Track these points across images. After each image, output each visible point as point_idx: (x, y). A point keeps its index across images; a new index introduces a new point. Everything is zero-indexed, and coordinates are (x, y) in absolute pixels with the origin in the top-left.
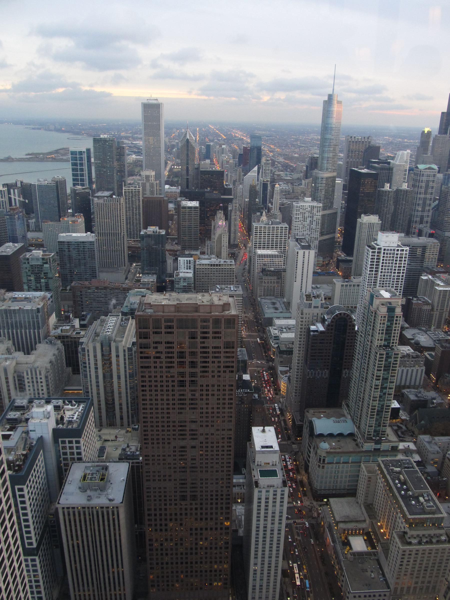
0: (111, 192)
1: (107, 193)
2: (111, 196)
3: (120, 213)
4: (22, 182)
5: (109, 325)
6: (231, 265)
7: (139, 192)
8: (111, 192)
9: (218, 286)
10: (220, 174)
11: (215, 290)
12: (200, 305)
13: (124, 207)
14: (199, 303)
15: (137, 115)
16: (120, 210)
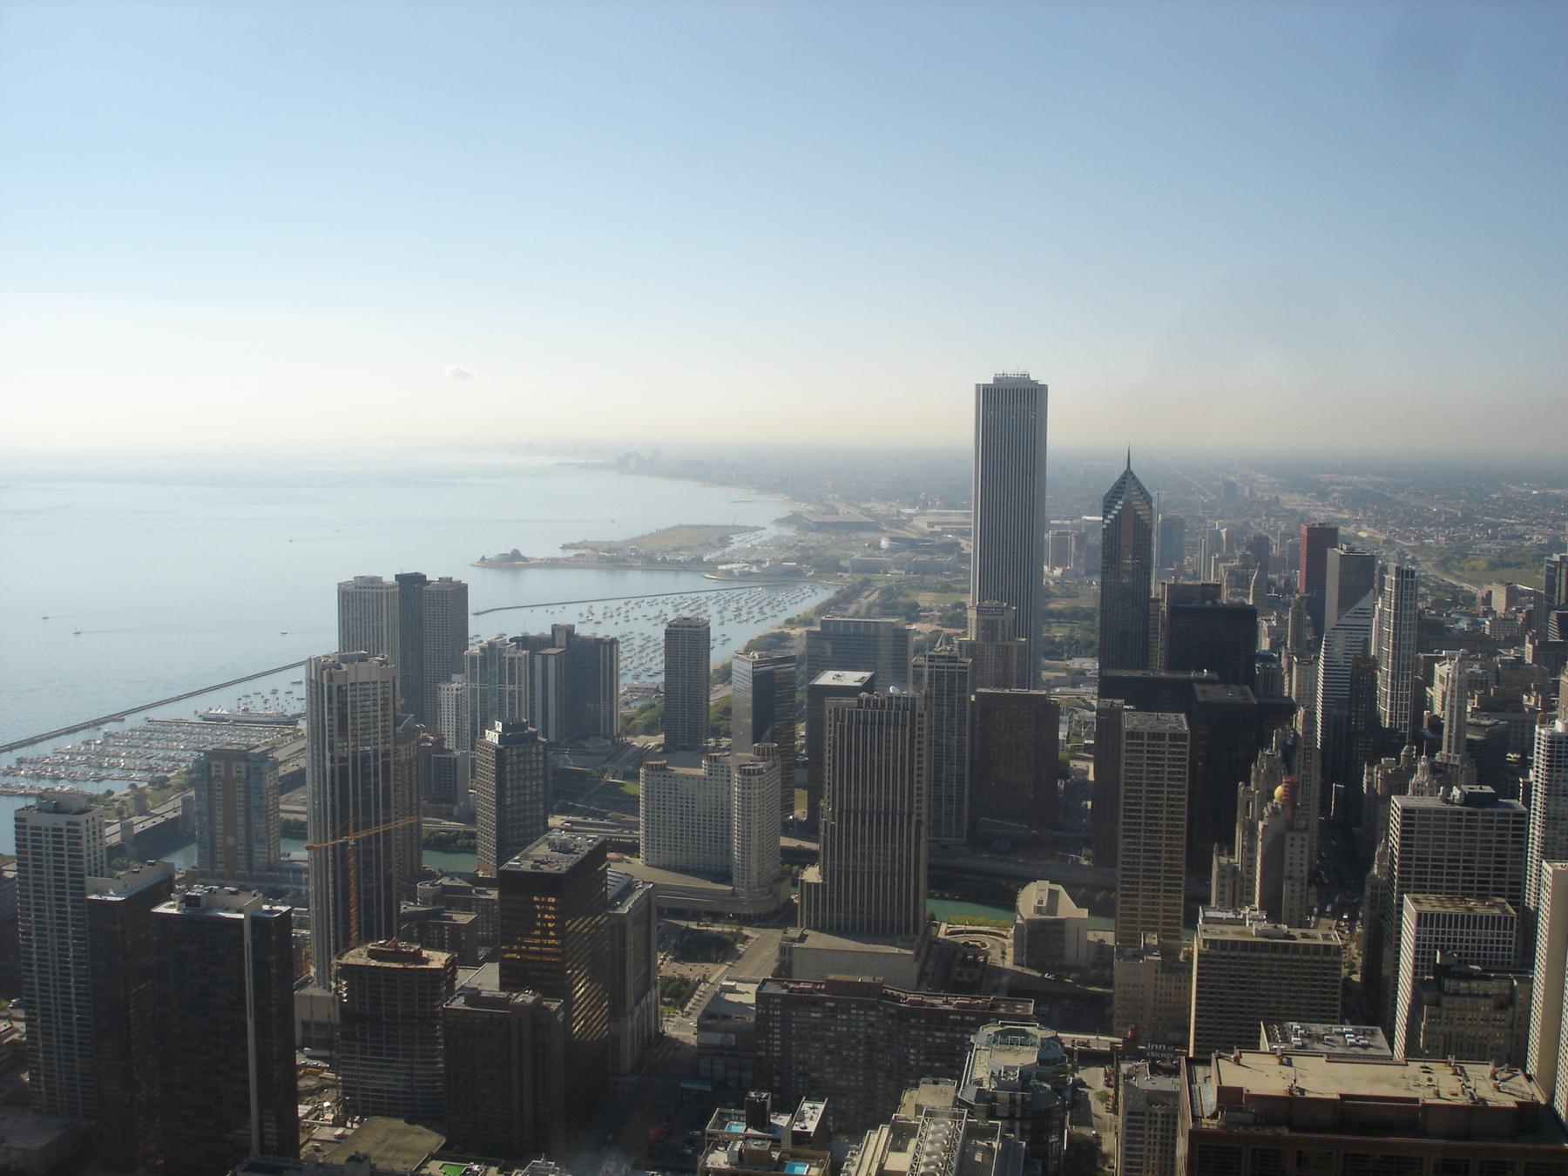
0: (868, 675)
1: (851, 678)
2: (869, 686)
3: (912, 746)
4: (569, 631)
5: (928, 1148)
6: (1327, 948)
7: (963, 676)
8: (868, 675)
9: (1296, 1026)
10: (1245, 618)
11: (1286, 1040)
12: (1427, 1107)
13: (925, 726)
14: (1426, 1096)
15: (954, 428)
16: (912, 737)
